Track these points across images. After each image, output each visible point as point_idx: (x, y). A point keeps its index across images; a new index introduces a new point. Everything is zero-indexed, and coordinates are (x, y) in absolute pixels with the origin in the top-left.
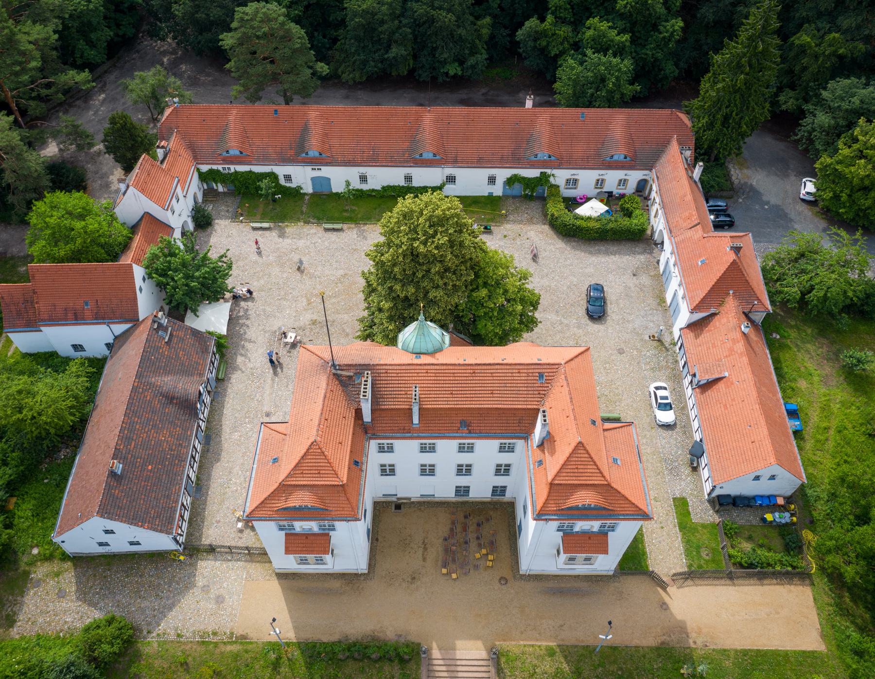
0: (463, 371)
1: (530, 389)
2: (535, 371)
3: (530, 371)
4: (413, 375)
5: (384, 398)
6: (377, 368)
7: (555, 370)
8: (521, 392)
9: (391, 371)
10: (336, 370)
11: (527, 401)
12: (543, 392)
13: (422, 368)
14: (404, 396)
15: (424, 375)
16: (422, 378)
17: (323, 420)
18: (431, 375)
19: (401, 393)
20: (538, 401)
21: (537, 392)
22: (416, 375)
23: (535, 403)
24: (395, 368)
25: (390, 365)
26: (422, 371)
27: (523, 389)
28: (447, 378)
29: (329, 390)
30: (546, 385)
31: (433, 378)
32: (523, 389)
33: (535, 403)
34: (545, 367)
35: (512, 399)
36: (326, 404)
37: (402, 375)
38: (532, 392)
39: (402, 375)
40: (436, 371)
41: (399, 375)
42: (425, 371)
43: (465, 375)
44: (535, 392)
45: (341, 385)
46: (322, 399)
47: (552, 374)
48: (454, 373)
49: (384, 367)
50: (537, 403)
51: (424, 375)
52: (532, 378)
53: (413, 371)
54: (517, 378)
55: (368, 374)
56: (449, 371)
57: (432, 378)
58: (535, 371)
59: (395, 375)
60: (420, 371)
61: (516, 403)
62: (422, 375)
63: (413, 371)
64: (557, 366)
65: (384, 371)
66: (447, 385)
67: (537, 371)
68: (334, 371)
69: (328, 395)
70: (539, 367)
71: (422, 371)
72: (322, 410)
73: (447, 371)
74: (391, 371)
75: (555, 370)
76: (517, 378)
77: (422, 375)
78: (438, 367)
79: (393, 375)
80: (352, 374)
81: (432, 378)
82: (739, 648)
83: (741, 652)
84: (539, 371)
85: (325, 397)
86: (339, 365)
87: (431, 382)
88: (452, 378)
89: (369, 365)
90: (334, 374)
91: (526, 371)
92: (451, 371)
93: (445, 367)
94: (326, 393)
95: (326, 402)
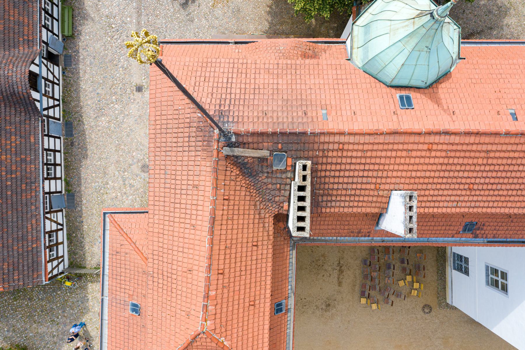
0: (510, 148)
4: (399, 154)
5: (331, 195)
6: (322, 139)
9: (351, 147)
10: (230, 145)
13: (422, 139)
14: (372, 193)
15: (423, 154)
16: (417, 161)
17: (214, 277)
18: (438, 154)
19: (368, 186)
22: (404, 154)
24: (362, 139)
25: (350, 134)
26: (421, 147)
28: (470, 161)
29: (220, 201)
31: (441, 161)
36: (217, 238)
37: (374, 154)
39: (374, 154)
40: (450, 147)
41: (369, 154)
42: (426, 147)
43: (512, 155)
45: (243, 174)
46: (207, 225)
48: (487, 151)
49: (337, 138)
51: (423, 154)
53: (401, 147)
55: (304, 168)
56: (480, 147)
57: (437, 161)
59: (359, 154)
60: (415, 147)
62: (419, 154)
63: (401, 147)
65: (336, 146)
66: (466, 174)
68: (226, 151)
69: (219, 213)
71: (421, 147)
72: (210, 258)
73: (474, 147)
74: (351, 147)
77: (419, 154)
78: (457, 139)
79: (354, 154)
80: (265, 153)
81: (437, 161)
85: (213, 220)
86: (237, 134)
87: (434, 168)
88: (480, 161)
89: (304, 134)
90: (227, 157)
92: (484, 148)
93: (472, 139)
94: (214, 210)
95: (217, 232)
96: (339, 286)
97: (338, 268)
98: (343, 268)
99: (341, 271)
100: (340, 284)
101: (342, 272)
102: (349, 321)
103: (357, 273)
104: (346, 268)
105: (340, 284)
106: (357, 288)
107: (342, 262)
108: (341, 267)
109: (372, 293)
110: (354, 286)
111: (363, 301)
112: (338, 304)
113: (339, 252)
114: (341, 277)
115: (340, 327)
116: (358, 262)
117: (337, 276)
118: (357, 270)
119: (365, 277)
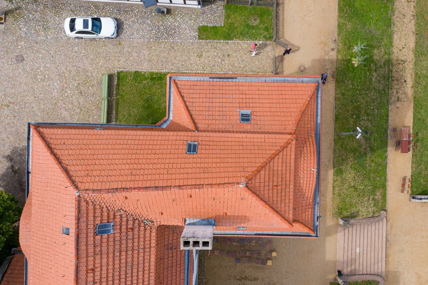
1: (124, 246)
2: (91, 242)
3: (91, 250)
7: (91, 207)
8: (129, 260)
11: (144, 248)
12: (131, 223)
20: (145, 230)
21: (130, 233)
23: (147, 235)
27: (123, 257)
30: (118, 220)
32: (123, 257)
33: (147, 235)
34: (83, 225)
35: (141, 273)
38: (130, 241)
44: (130, 237)
47: (98, 211)
50: (148, 232)
52: (104, 244)
54: (104, 272)
58: (91, 242)
61: (147, 265)
64: (83, 204)
67: (91, 239)
70: (83, 236)
75: (91, 207)
76: (104, 272)
82: (337, 13)
83: (341, 13)
84: (91, 235)
91: (91, 259)
96: (258, 279)
97: (243, 280)
98: (243, 277)
99: (246, 278)
100: (256, 279)
101: (246, 277)
102: (287, 272)
103: (247, 265)
104: (243, 274)
105: (256, 279)
106: (260, 265)
107: (238, 278)
108: (242, 278)
109: (263, 252)
110: (258, 267)
111: (269, 263)
112: (273, 281)
113: (230, 280)
114: (250, 278)
115: (291, 280)
116: (238, 264)
117: (249, 282)
118: (245, 265)
119: (250, 259)
